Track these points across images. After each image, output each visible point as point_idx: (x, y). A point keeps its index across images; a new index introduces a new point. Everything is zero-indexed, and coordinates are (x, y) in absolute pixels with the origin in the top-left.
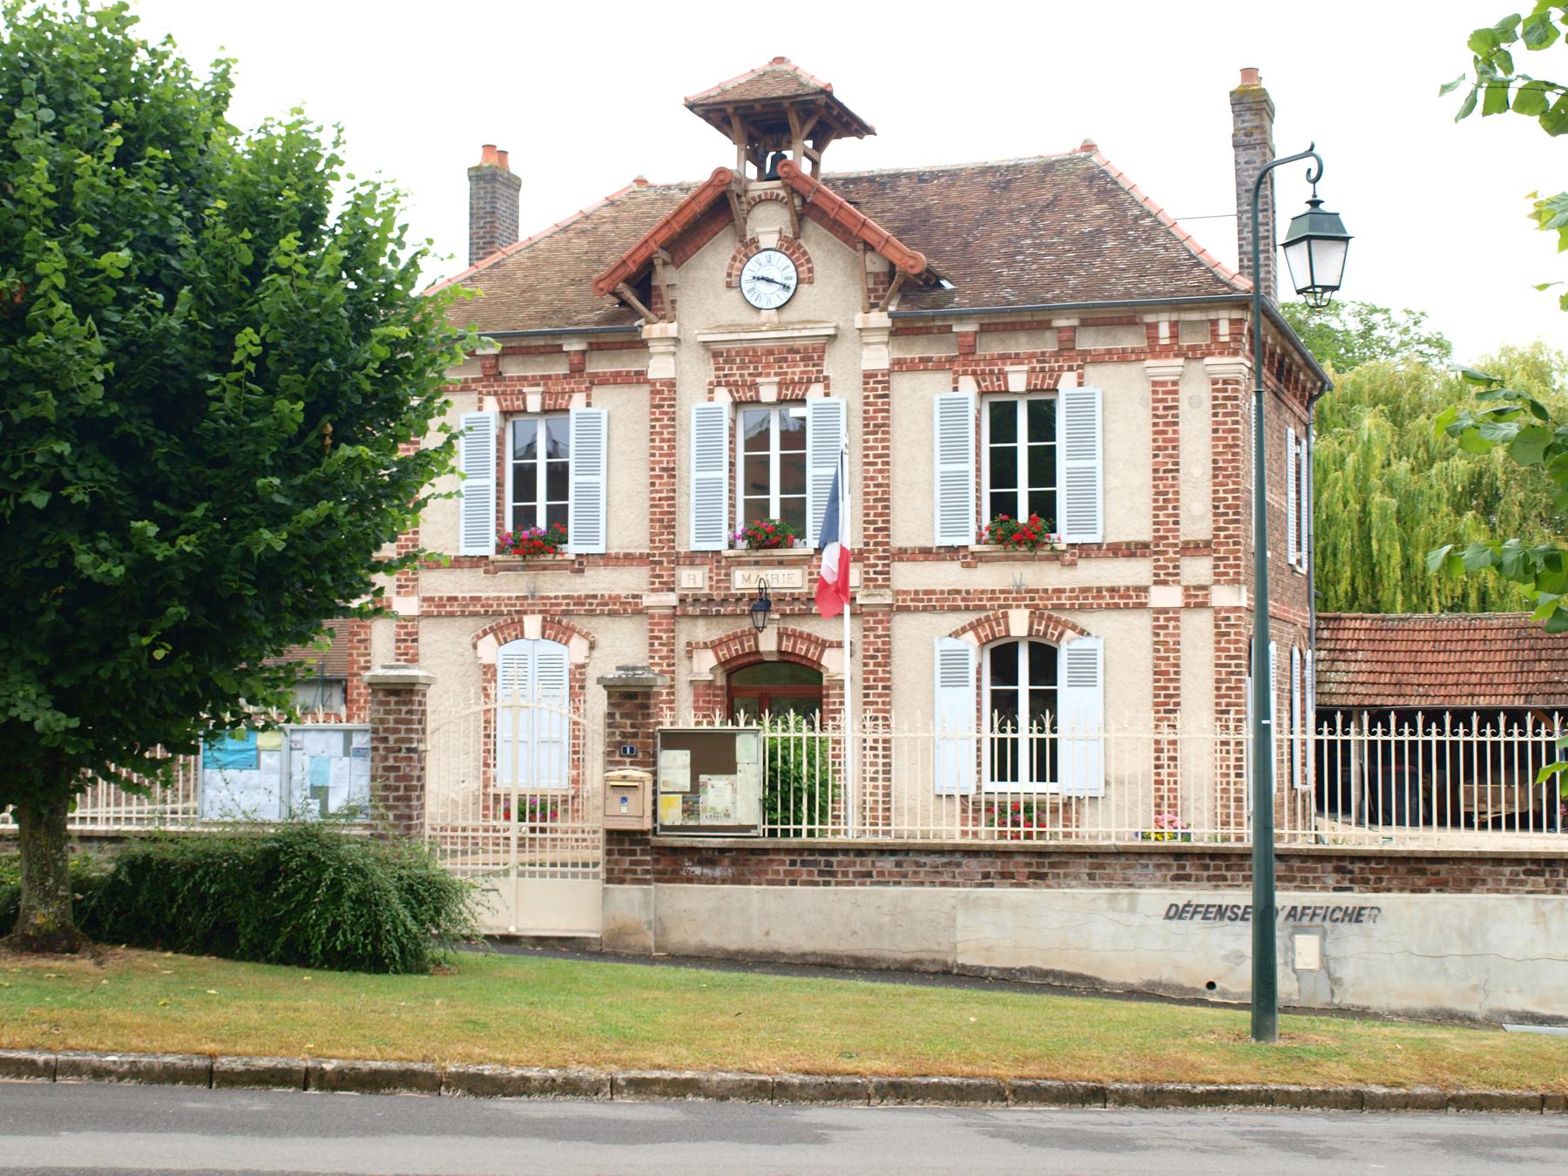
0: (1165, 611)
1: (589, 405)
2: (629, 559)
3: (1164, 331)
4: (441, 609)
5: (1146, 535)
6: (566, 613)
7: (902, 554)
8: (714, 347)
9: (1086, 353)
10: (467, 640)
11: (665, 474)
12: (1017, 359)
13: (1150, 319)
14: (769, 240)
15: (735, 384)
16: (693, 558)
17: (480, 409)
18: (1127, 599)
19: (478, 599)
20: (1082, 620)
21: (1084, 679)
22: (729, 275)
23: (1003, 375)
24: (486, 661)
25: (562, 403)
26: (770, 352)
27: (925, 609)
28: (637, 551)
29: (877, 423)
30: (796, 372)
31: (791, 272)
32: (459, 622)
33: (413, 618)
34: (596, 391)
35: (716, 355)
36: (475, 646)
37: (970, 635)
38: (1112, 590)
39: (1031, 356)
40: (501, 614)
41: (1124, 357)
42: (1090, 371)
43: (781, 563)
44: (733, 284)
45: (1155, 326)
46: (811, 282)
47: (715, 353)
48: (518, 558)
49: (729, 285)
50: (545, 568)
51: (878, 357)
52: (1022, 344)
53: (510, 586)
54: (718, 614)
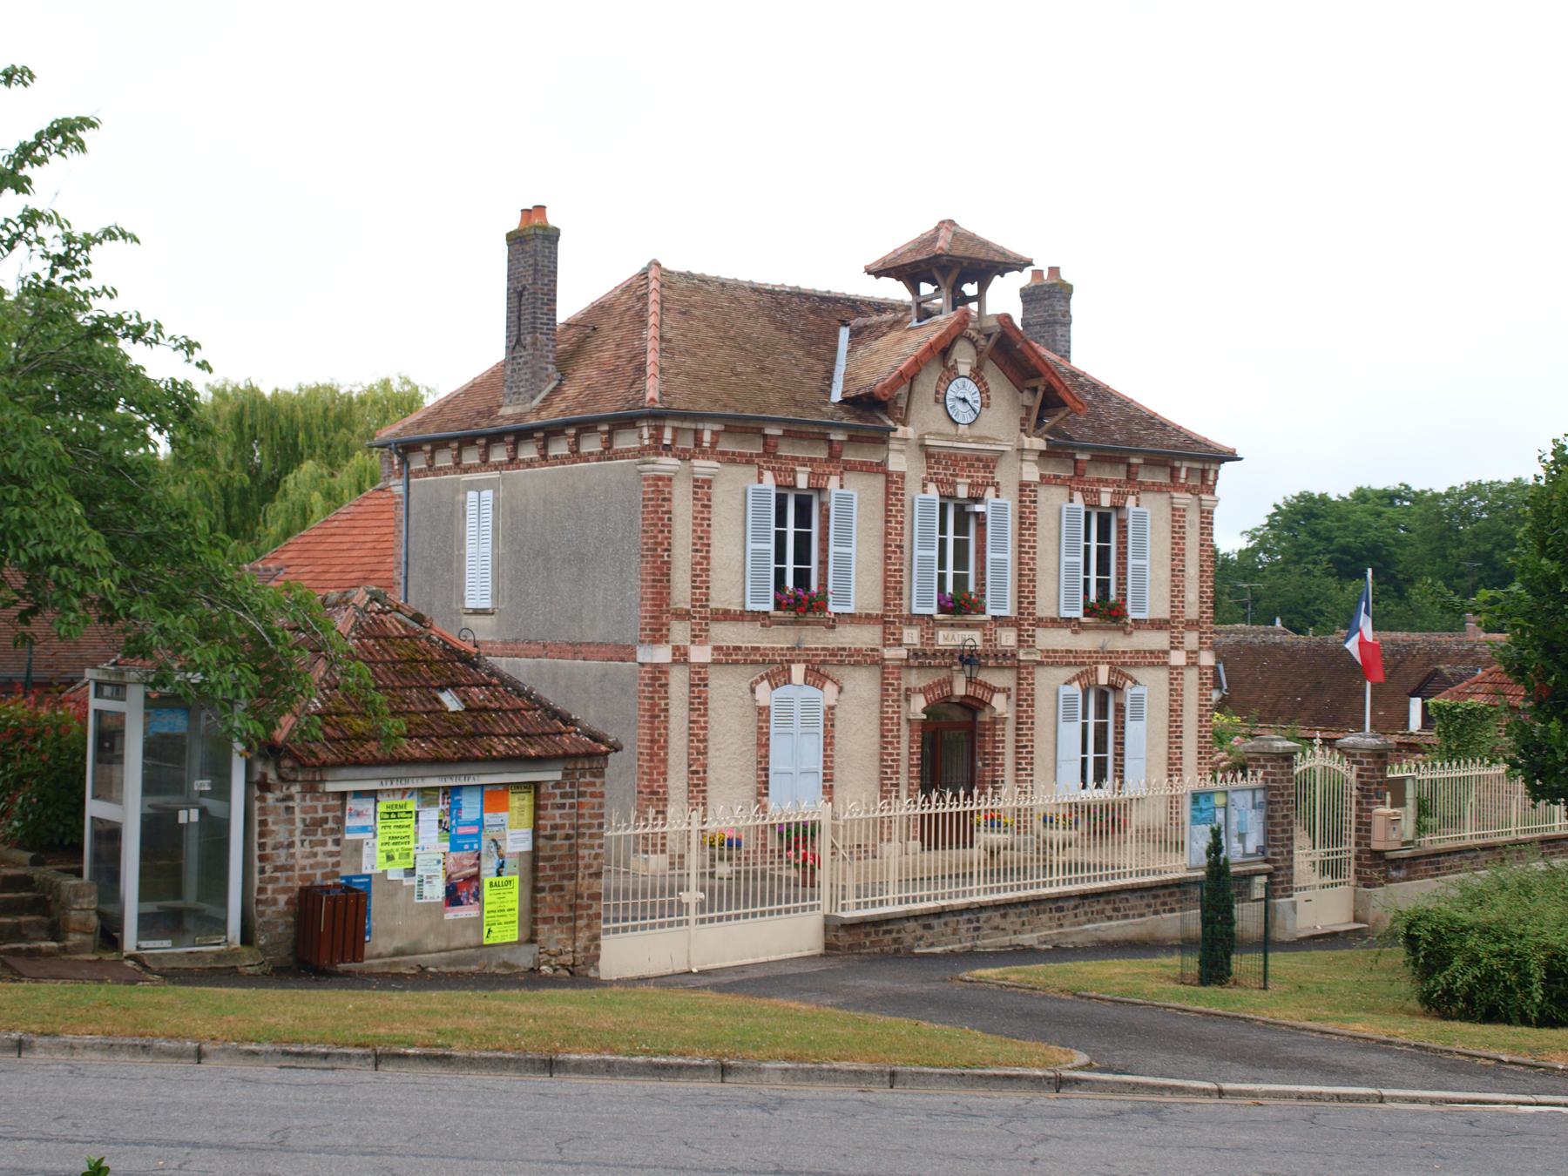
0: (1176, 667)
1: (841, 487)
2: (868, 619)
3: (1183, 474)
4: (728, 657)
5: (1167, 616)
6: (824, 662)
7: (1041, 623)
8: (931, 450)
9: (1142, 483)
10: (746, 685)
11: (893, 551)
12: (1106, 483)
13: (1177, 464)
14: (964, 369)
15: (941, 481)
16: (912, 620)
17: (760, 481)
18: (1156, 659)
19: (757, 649)
20: (1134, 673)
21: (1138, 717)
22: (937, 392)
23: (1098, 493)
24: (762, 703)
25: (822, 483)
26: (965, 459)
27: (1052, 664)
28: (875, 612)
29: (1026, 522)
30: (979, 476)
31: (977, 397)
32: (740, 669)
33: (704, 665)
34: (846, 476)
35: (929, 456)
36: (753, 691)
37: (1076, 684)
38: (1151, 652)
39: (1114, 481)
40: (775, 662)
41: (1158, 488)
42: (1142, 496)
43: (968, 626)
44: (940, 400)
45: (1179, 469)
46: (988, 406)
47: (928, 453)
48: (793, 614)
49: (937, 401)
50: (808, 624)
51: (1031, 473)
52: (1107, 473)
53: (779, 639)
54: (930, 666)
